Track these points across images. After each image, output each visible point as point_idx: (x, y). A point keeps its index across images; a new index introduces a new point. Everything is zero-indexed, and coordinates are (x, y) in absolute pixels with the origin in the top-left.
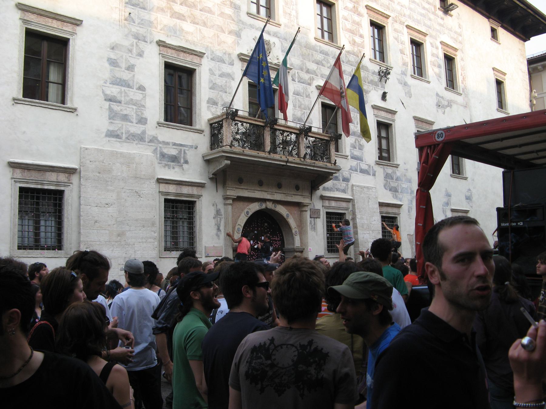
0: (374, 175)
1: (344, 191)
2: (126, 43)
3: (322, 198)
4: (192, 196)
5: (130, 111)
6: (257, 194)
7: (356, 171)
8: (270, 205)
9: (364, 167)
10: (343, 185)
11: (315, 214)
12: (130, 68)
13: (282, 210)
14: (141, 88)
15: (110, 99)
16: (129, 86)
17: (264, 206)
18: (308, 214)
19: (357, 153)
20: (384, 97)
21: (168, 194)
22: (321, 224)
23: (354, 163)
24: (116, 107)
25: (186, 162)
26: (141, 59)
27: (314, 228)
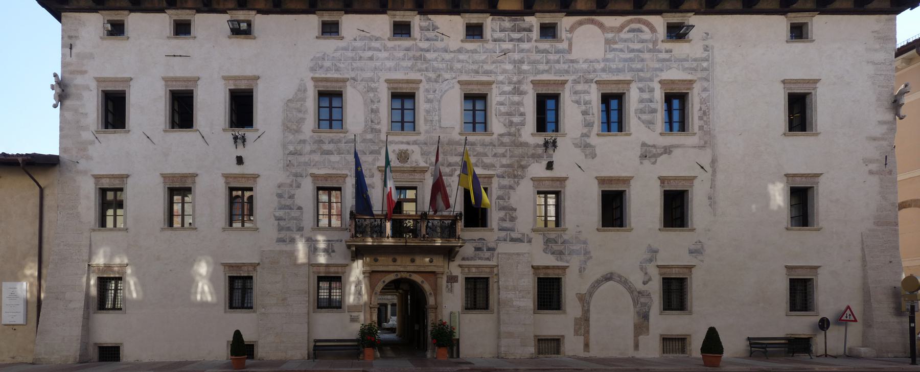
0: (530, 241)
1: (488, 259)
2: (289, 181)
3: (460, 266)
4: (338, 273)
5: (293, 224)
6: (391, 268)
7: (505, 240)
8: (404, 275)
9: (514, 235)
10: (487, 254)
11: (452, 279)
12: (292, 197)
13: (417, 278)
14: (300, 208)
15: (279, 219)
16: (291, 209)
17: (399, 277)
18: (445, 279)
19: (507, 224)
20: (550, 166)
21: (319, 273)
22: (459, 288)
23: (503, 234)
24: (282, 223)
25: (333, 251)
26: (299, 190)
27: (451, 290)
